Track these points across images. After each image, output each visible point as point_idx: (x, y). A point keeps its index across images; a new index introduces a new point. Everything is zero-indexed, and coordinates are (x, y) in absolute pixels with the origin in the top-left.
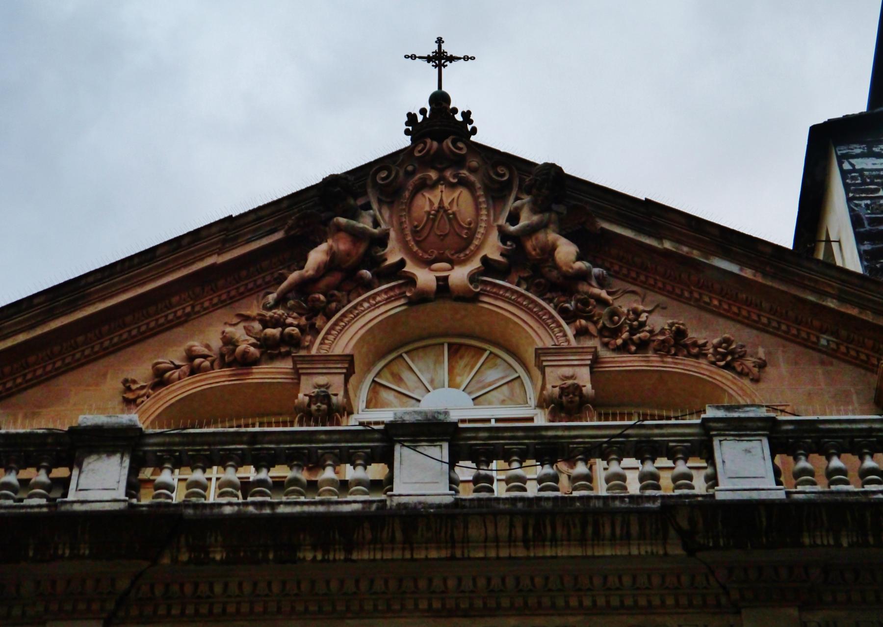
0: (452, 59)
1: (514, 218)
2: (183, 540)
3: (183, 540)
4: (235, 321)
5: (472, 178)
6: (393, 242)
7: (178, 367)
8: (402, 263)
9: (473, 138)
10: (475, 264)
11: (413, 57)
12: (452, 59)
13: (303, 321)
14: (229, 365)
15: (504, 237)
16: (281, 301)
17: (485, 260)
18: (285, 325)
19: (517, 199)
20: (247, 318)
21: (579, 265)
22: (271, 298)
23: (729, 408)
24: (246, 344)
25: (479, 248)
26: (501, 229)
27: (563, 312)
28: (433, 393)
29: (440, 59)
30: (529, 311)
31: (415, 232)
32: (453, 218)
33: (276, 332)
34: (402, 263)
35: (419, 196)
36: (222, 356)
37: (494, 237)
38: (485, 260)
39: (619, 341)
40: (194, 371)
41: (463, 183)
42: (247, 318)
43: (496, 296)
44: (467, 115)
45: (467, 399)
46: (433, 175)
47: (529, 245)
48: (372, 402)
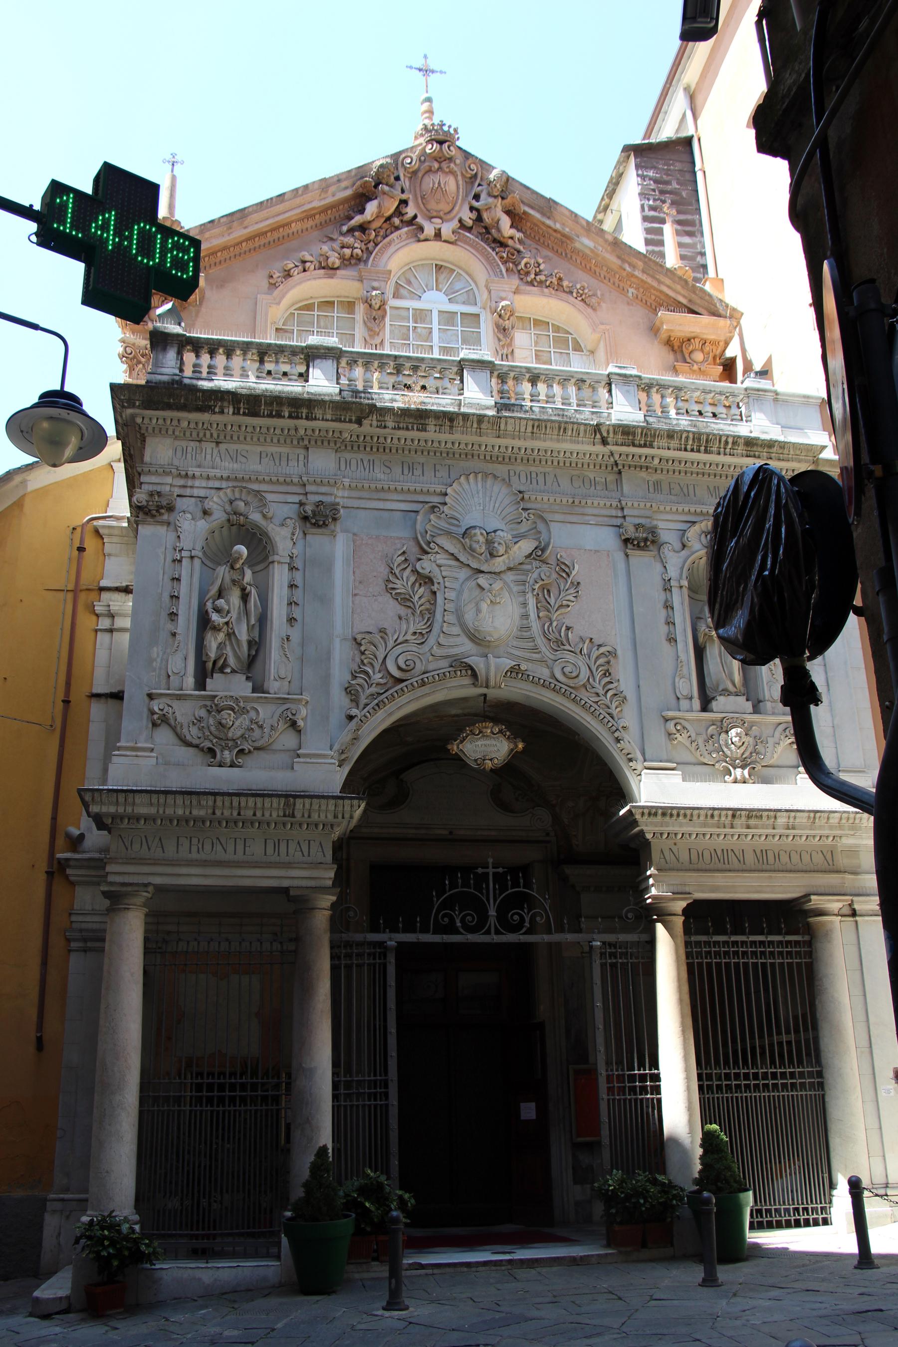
0: (433, 72)
1: (477, 197)
2: (375, 417)
3: (375, 417)
4: (325, 240)
5: (456, 169)
6: (411, 203)
7: (296, 266)
8: (415, 217)
9: (458, 143)
10: (455, 224)
11: (411, 67)
12: (433, 72)
13: (364, 247)
14: (324, 268)
15: (472, 209)
16: (351, 231)
17: (460, 221)
18: (353, 248)
19: (479, 185)
20: (332, 239)
21: (513, 232)
22: (345, 228)
23: (620, 367)
24: (334, 259)
25: (458, 213)
26: (469, 203)
27: (502, 258)
28: (427, 292)
29: (426, 71)
30: (477, 250)
31: (423, 198)
32: (444, 193)
33: (347, 252)
34: (415, 217)
35: (426, 177)
36: (320, 263)
37: (466, 208)
38: (460, 221)
39: (529, 279)
40: (305, 271)
41: (452, 172)
42: (332, 239)
43: (465, 242)
44: (456, 130)
45: (446, 299)
46: (436, 165)
47: (485, 216)
48: (396, 295)
